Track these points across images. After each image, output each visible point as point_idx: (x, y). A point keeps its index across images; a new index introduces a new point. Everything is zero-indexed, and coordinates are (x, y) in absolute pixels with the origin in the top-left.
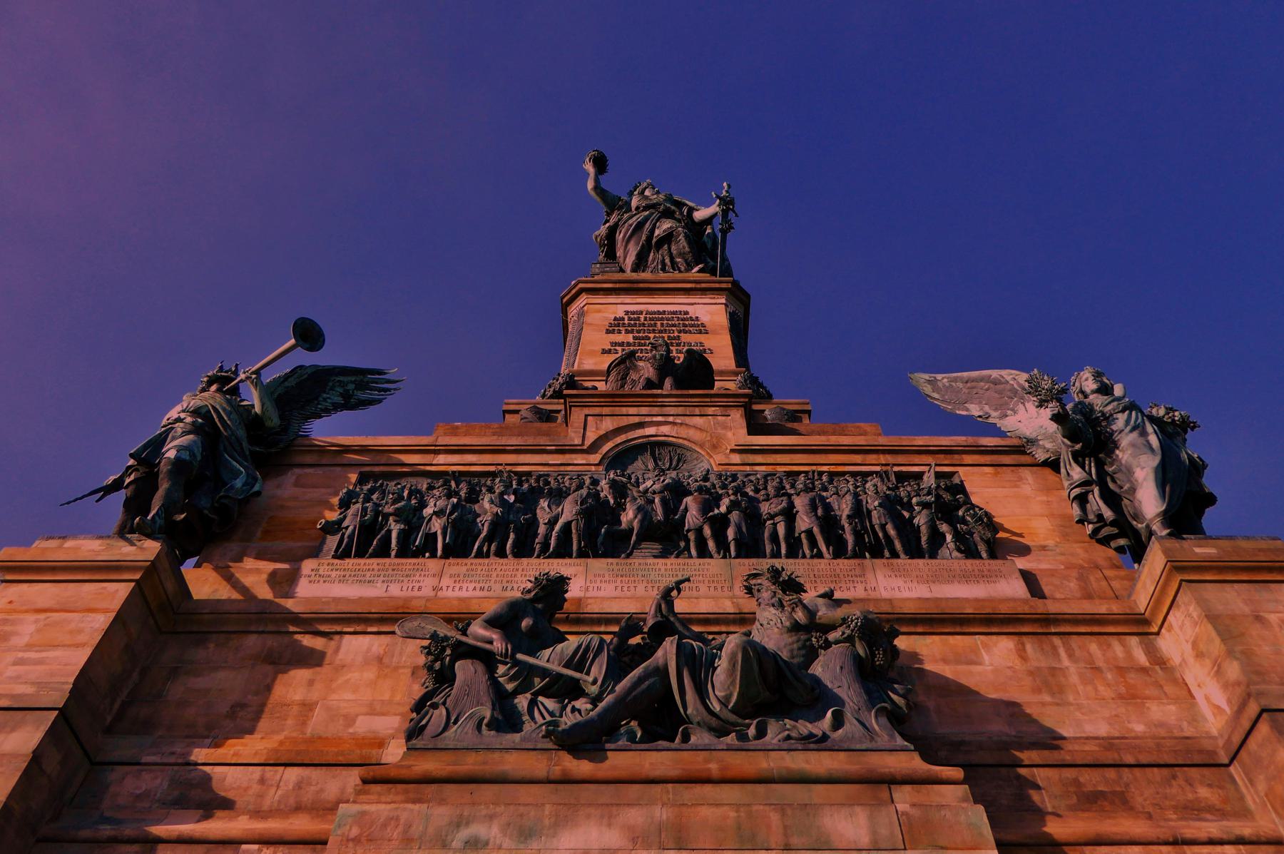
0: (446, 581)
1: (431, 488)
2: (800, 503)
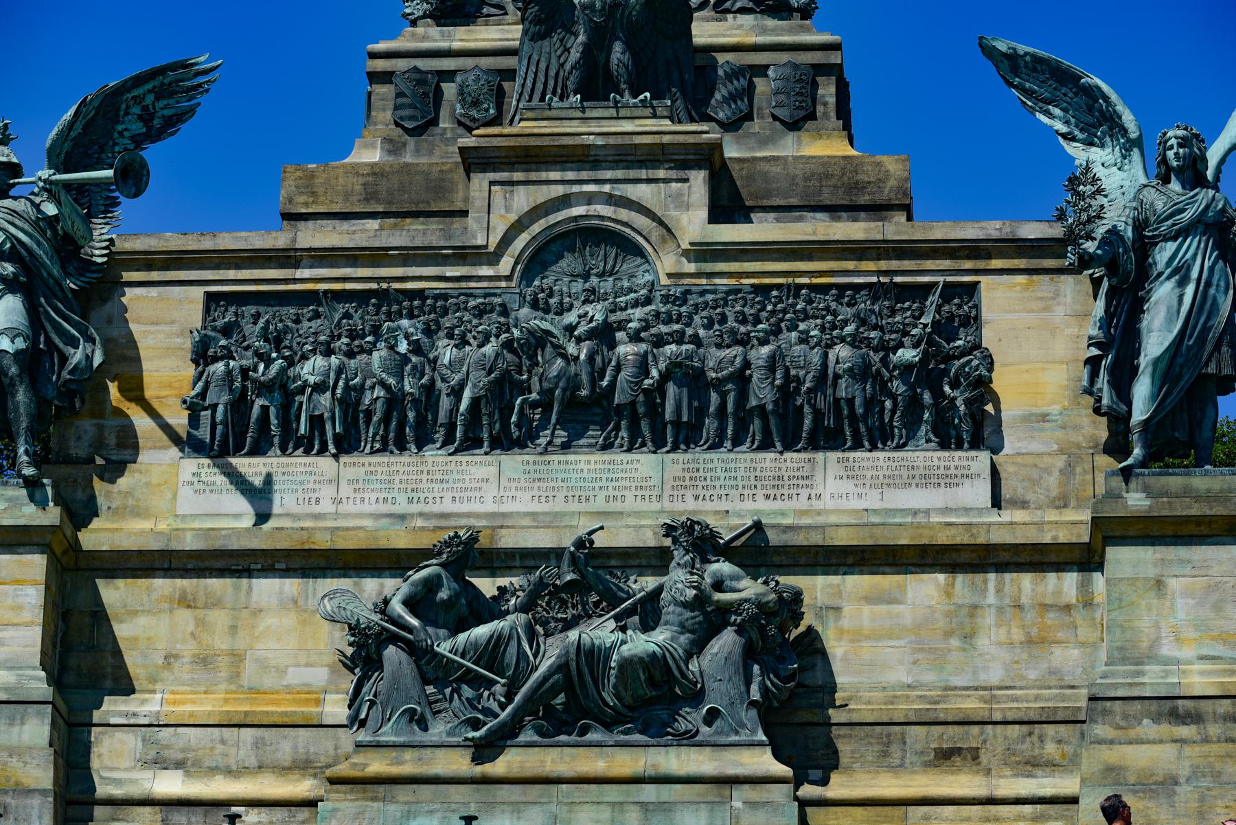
0: (346, 490)
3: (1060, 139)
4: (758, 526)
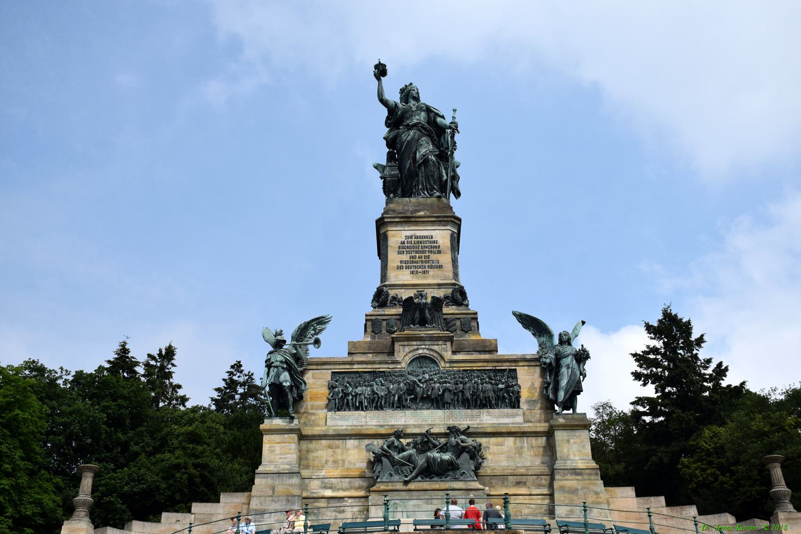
0: (368, 419)
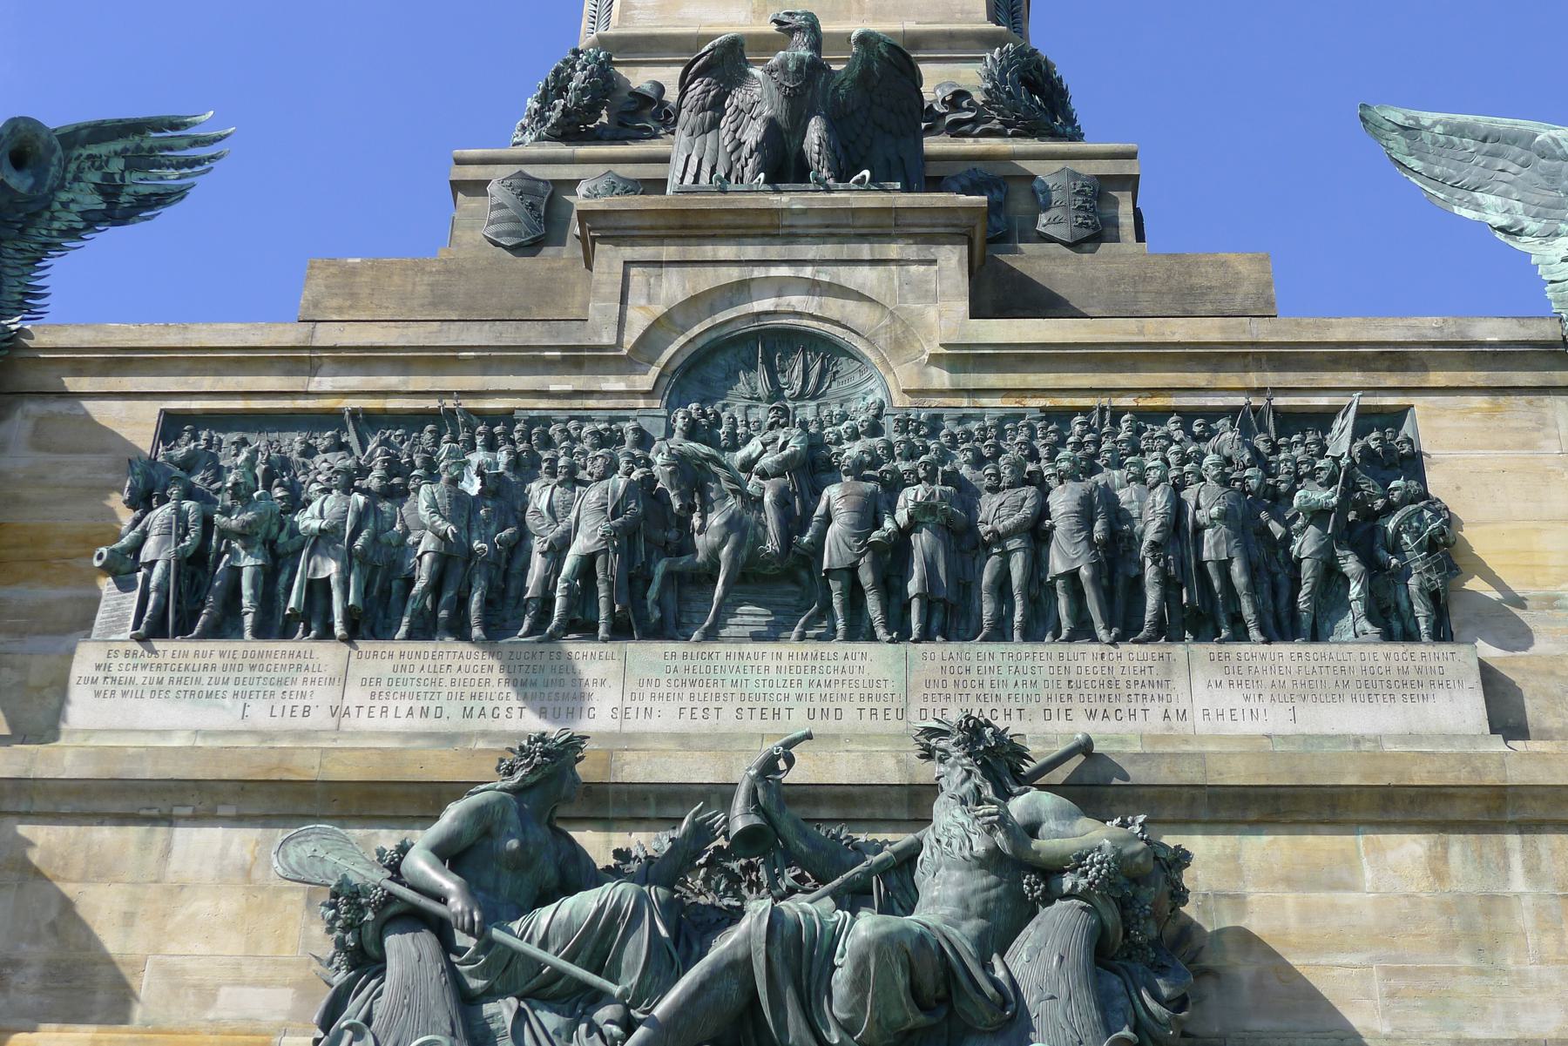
0: (356, 695)
1: (309, 451)
2: (1062, 501)
3: (1499, 235)
4: (1085, 747)
